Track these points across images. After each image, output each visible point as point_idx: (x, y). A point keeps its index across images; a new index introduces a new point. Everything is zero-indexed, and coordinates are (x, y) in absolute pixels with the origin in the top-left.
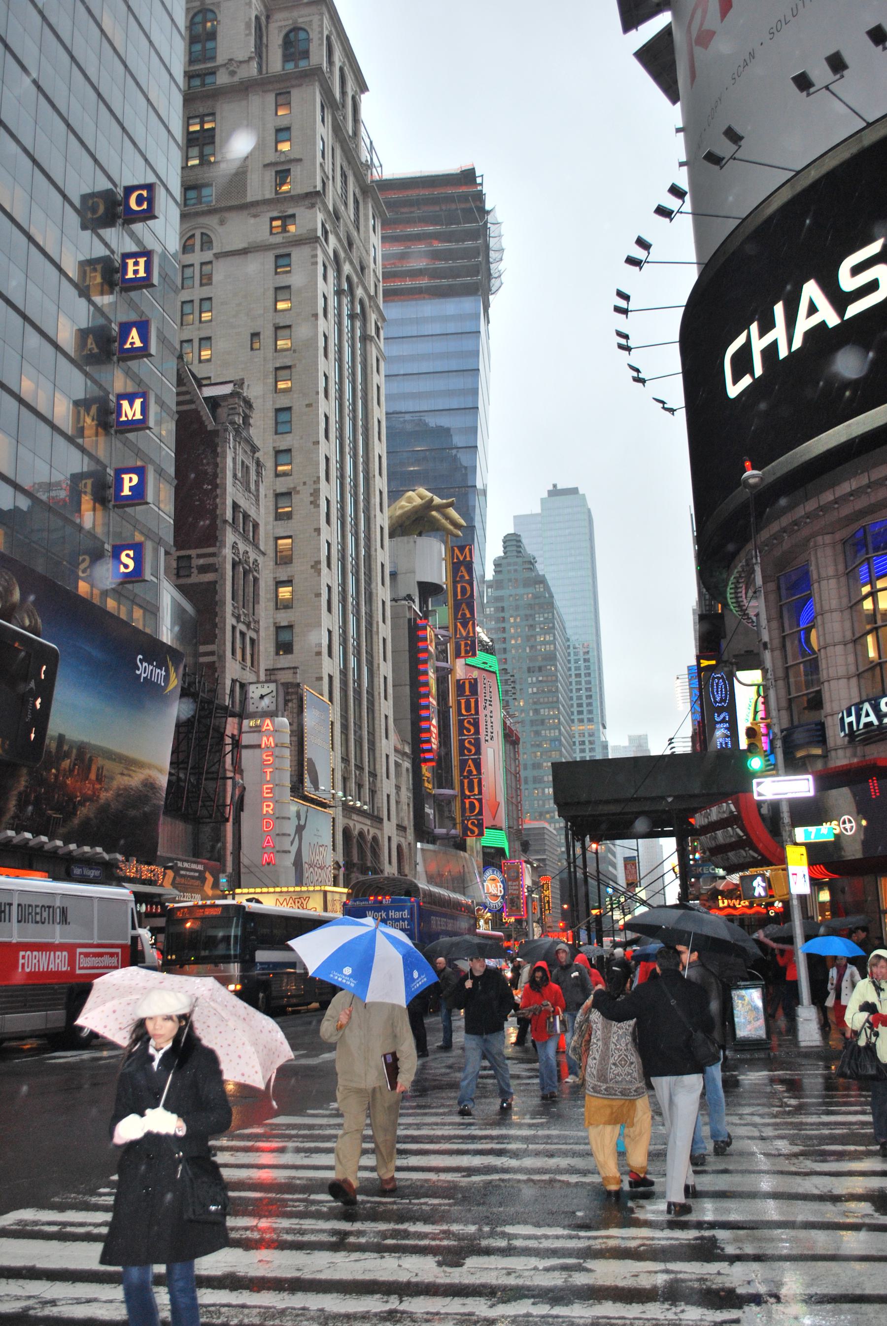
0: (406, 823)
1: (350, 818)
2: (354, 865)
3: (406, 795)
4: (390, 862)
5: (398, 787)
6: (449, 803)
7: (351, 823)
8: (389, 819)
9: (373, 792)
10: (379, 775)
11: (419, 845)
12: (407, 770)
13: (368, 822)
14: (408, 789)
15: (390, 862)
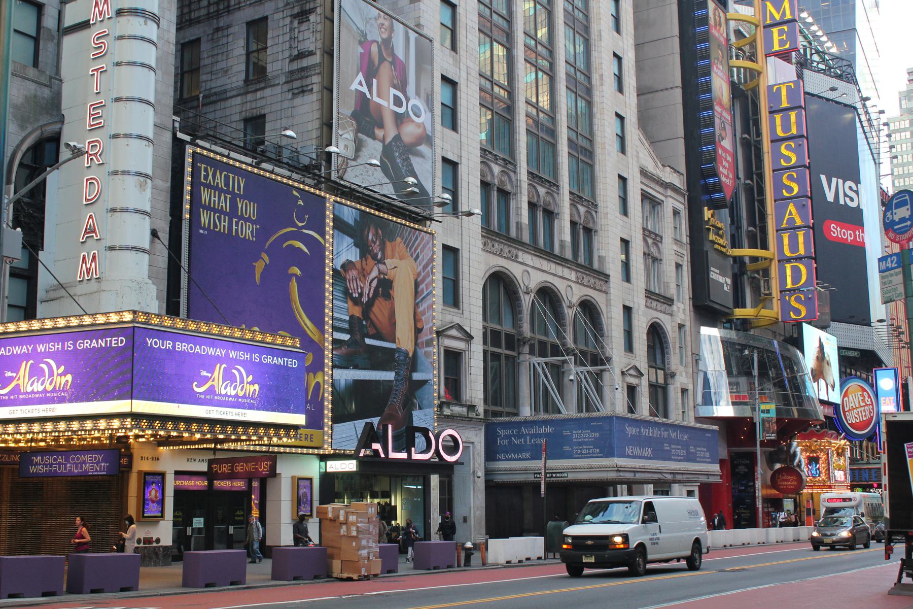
0: (672, 292)
1: (514, 259)
2: (523, 341)
3: (674, 250)
4: (629, 347)
5: (652, 236)
6: (766, 272)
7: (515, 270)
8: (627, 278)
9: (585, 232)
10: (601, 204)
11: (711, 333)
12: (676, 213)
13: (573, 276)
14: (677, 241)
15: (629, 347)
